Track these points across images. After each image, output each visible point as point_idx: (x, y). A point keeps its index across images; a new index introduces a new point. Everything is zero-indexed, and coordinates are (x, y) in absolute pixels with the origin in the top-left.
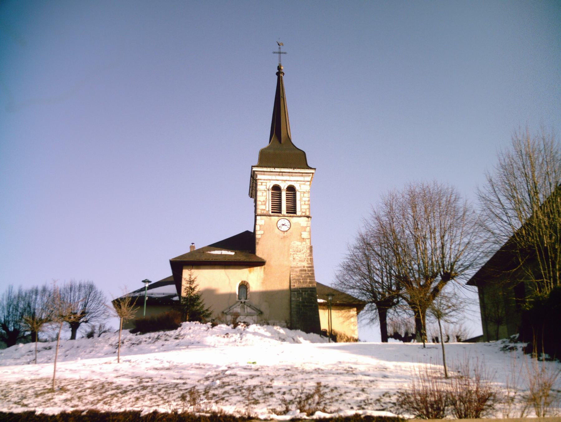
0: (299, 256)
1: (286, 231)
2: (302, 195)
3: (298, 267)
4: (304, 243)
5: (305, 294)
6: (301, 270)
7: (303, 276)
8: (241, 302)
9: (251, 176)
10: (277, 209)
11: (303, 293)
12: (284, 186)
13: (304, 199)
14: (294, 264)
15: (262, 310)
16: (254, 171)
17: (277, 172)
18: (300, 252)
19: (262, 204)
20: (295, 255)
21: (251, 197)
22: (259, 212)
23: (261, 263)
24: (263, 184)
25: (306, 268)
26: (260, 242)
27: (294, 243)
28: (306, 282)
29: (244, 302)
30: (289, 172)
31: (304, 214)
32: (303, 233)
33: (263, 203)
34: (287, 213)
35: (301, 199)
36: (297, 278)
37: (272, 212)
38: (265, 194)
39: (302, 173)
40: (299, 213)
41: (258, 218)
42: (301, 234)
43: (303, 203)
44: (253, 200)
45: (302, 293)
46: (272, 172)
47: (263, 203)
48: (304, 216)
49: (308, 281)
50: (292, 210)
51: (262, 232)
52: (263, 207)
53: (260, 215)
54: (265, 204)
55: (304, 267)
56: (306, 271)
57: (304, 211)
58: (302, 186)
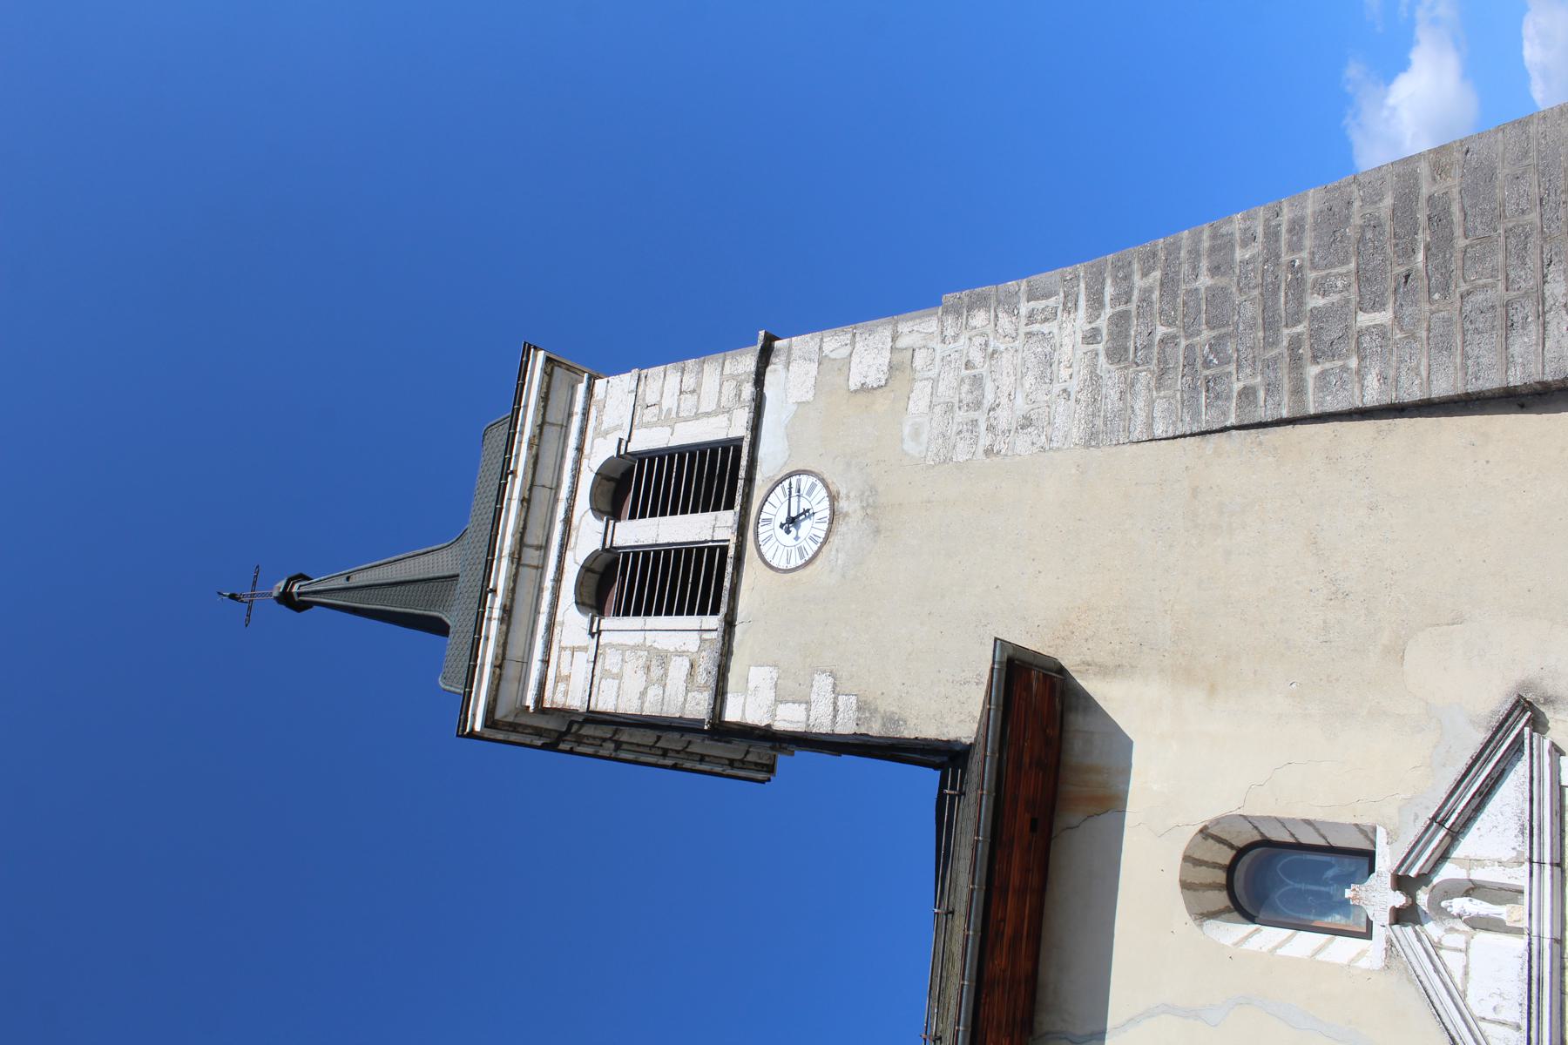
0: (1012, 387)
1: (833, 498)
2: (649, 415)
3: (1094, 379)
4: (920, 359)
5: (1322, 288)
6: (1117, 353)
7: (1161, 330)
8: (1402, 916)
9: (551, 747)
10: (692, 583)
11: (1315, 301)
12: (589, 535)
13: (669, 402)
14: (1068, 421)
15: (1493, 700)
16: (490, 721)
17: (514, 578)
18: (977, 381)
19: (662, 681)
20: (1004, 418)
21: (770, 769)
22: (697, 707)
23: (1036, 701)
24: (564, 672)
25: (1103, 323)
26: (887, 705)
27: (916, 434)
28: (1217, 297)
29: (1401, 882)
30: (526, 502)
31: (748, 390)
32: (854, 383)
33: (656, 672)
34: (730, 506)
35: (670, 420)
36: (1179, 382)
37: (715, 611)
38: (610, 661)
39: (541, 426)
40: (738, 427)
41: (732, 714)
42: (864, 389)
43: (689, 400)
44: (782, 760)
45: (1317, 315)
46: (507, 611)
47: (656, 672)
48: (759, 381)
49: (1205, 281)
50: (713, 474)
51: (823, 683)
52: (678, 669)
53: (720, 694)
54: (664, 658)
55: (1092, 337)
56: (1120, 320)
57: (729, 388)
58: (609, 420)
